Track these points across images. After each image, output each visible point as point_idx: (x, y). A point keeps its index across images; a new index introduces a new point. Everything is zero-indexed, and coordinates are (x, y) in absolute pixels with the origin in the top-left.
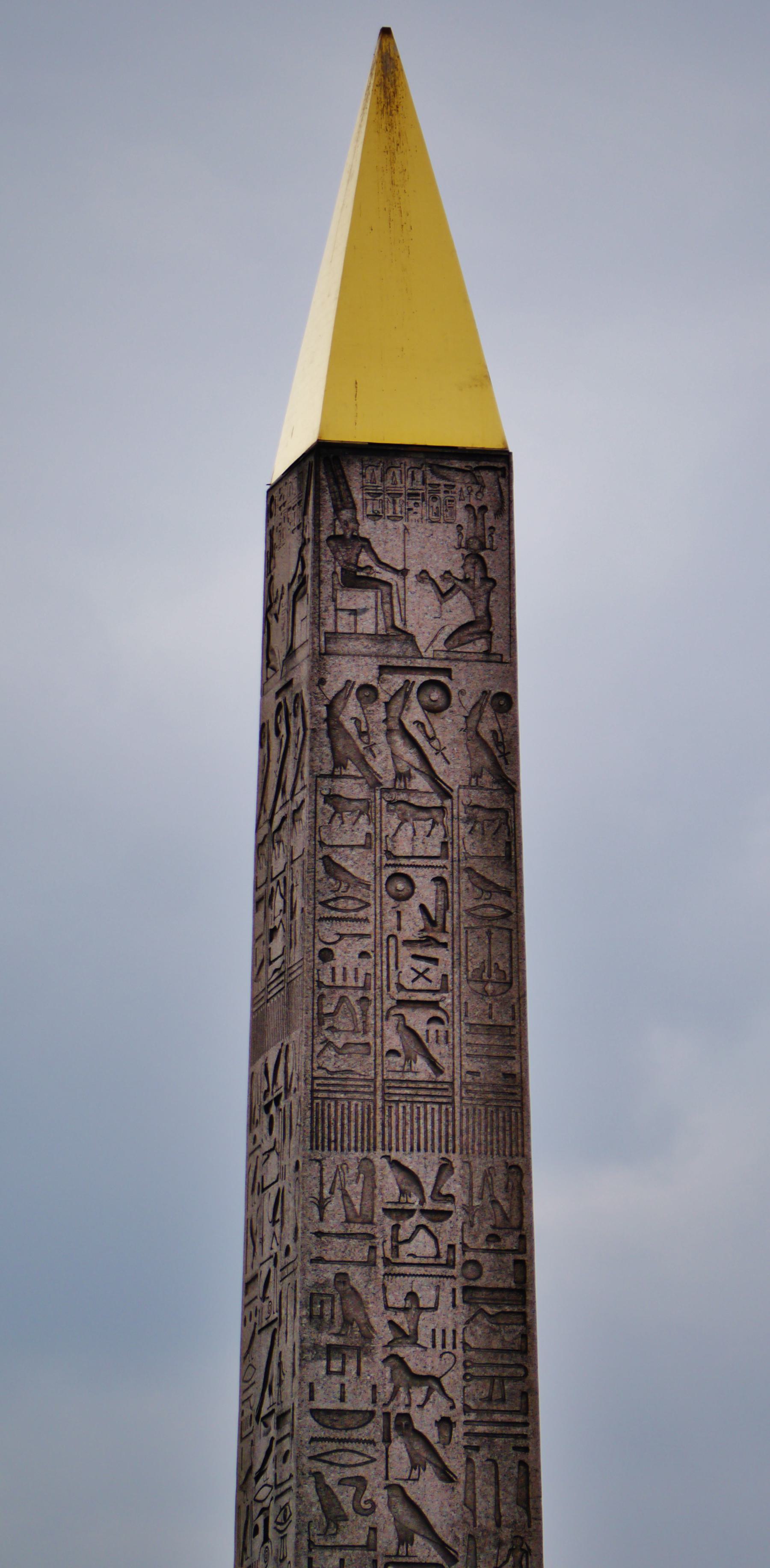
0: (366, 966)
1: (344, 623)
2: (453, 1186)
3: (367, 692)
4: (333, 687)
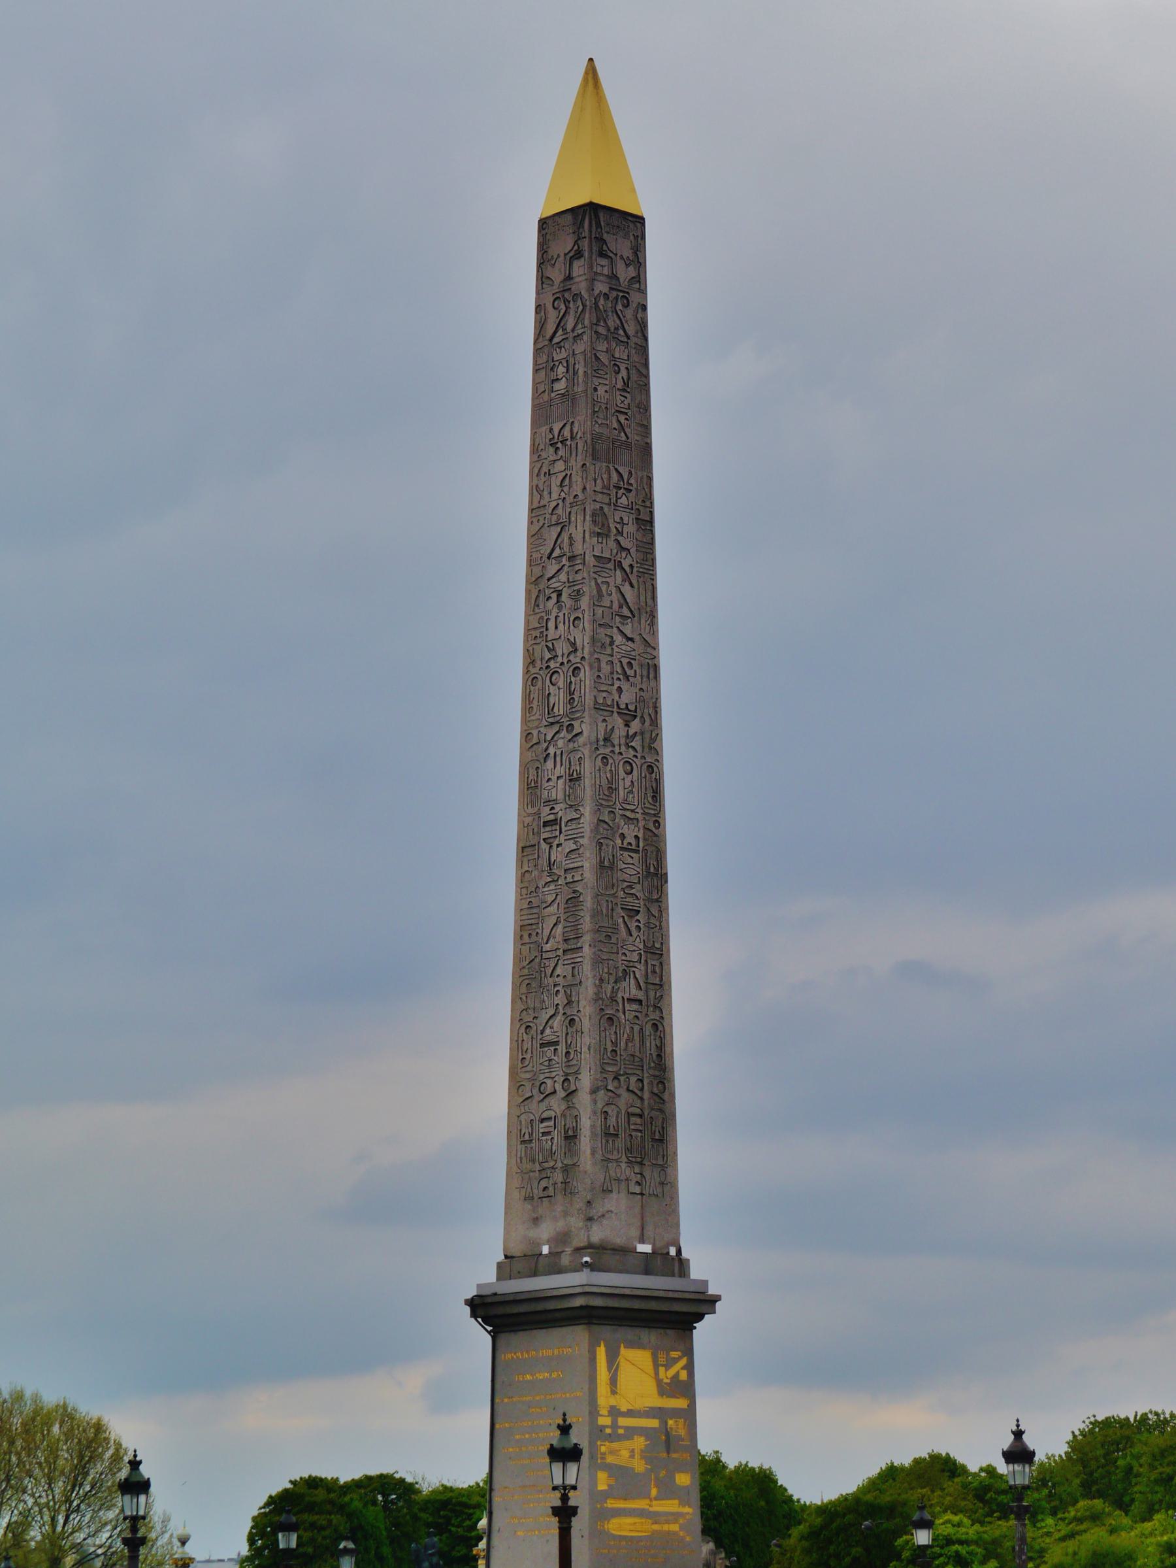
0: (607, 395)
1: (599, 269)
2: (632, 481)
3: (606, 296)
4: (596, 292)
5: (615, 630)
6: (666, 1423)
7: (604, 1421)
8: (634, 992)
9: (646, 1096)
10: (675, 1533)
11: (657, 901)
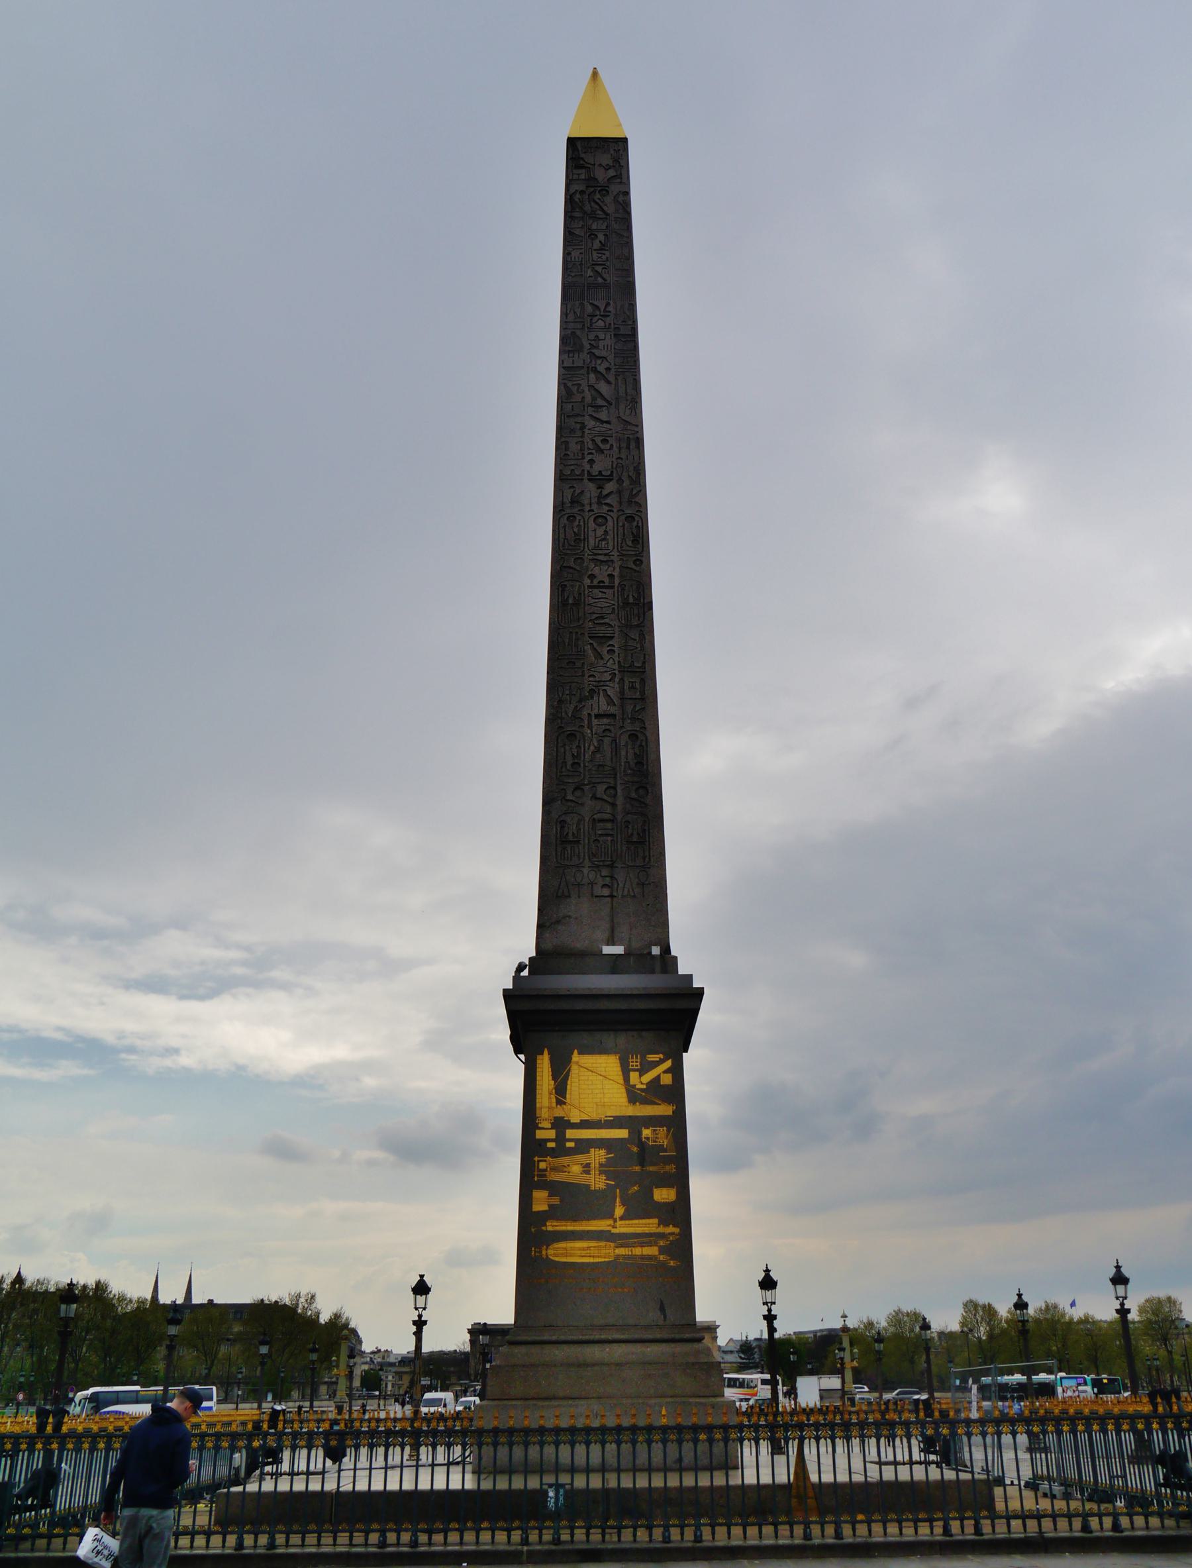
2: (610, 308)
3: (582, 192)
4: (572, 191)
5: (587, 417)
6: (640, 1133)
7: (545, 1133)
8: (604, 707)
9: (620, 801)
10: (650, 1258)
11: (638, 626)
